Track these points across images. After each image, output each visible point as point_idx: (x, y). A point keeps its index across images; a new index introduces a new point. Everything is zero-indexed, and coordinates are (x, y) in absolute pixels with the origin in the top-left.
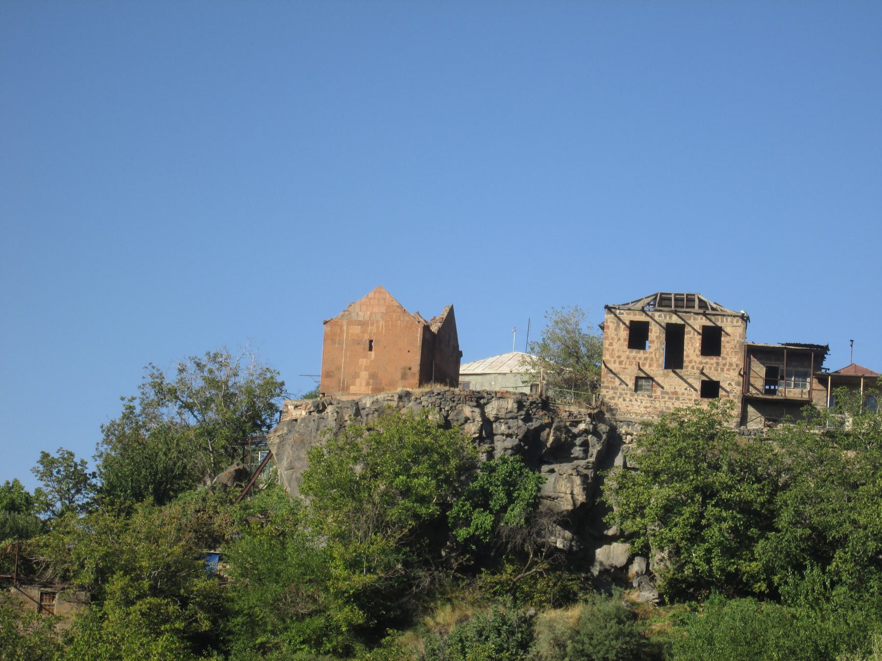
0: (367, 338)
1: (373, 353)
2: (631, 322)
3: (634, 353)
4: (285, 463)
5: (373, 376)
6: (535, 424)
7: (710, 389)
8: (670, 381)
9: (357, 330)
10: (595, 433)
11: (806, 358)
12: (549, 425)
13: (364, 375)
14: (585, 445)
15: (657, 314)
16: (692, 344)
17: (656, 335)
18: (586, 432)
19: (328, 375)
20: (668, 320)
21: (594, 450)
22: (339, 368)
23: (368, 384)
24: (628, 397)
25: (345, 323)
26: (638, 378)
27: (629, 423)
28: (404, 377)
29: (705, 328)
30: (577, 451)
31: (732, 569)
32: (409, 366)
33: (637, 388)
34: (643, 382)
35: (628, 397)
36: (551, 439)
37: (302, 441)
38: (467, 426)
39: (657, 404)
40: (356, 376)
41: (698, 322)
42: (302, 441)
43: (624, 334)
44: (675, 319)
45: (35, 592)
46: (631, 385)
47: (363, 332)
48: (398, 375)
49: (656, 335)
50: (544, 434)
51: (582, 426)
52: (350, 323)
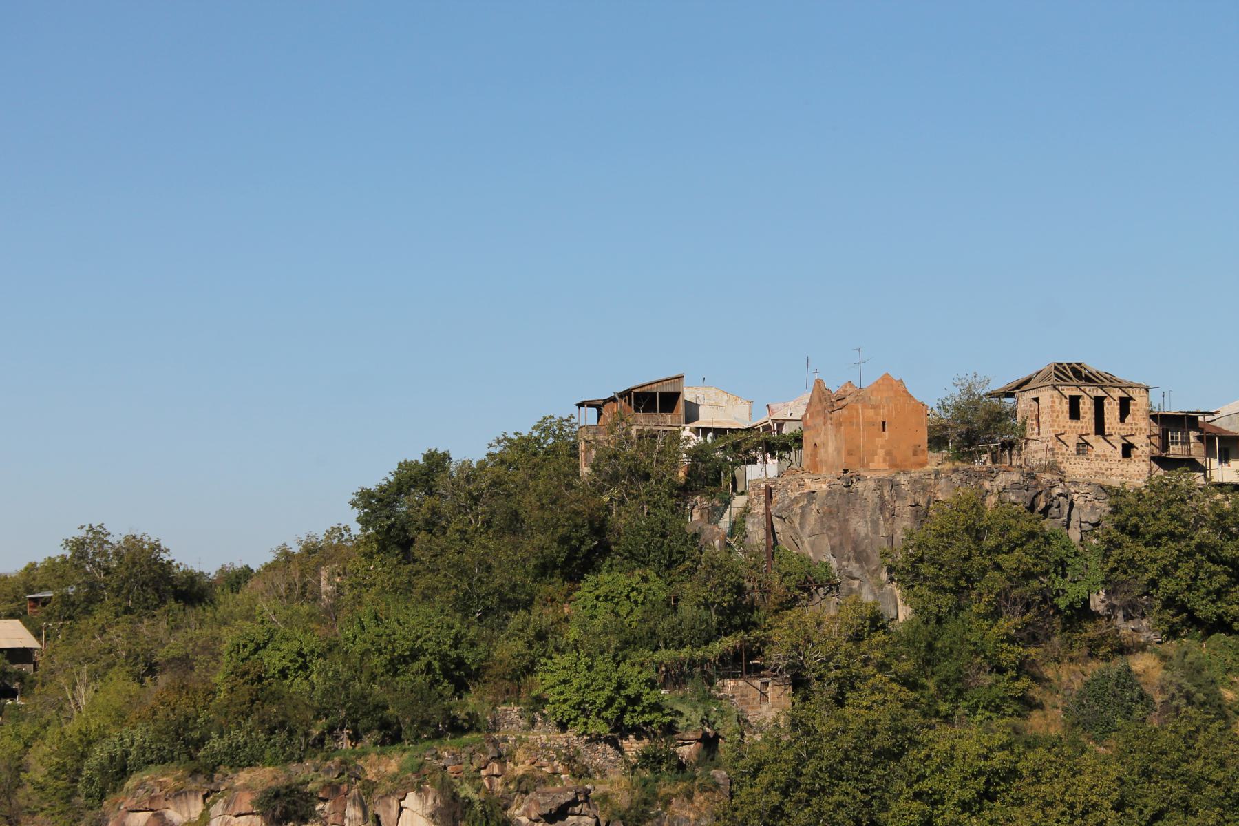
0: (880, 420)
1: (886, 433)
2: (1071, 397)
3: (1074, 423)
4: (807, 530)
5: (888, 453)
6: (1032, 493)
7: (1127, 450)
8: (1099, 445)
9: (871, 412)
10: (1066, 497)
11: (1187, 421)
12: (1040, 493)
13: (881, 452)
14: (1059, 506)
15: (1087, 389)
16: (1112, 411)
17: (1087, 407)
18: (1060, 495)
19: (850, 453)
20: (1096, 394)
21: (1067, 508)
22: (859, 447)
23: (885, 460)
24: (1073, 461)
25: (860, 406)
26: (1078, 444)
27: (1075, 483)
28: (915, 454)
29: (1121, 399)
30: (1054, 511)
31: (1220, 611)
32: (917, 443)
33: (1078, 453)
34: (1083, 447)
35: (1073, 461)
36: (1043, 505)
37: (831, 513)
38: (987, 498)
39: (1093, 466)
40: (874, 453)
41: (1117, 394)
42: (831, 513)
43: (1066, 407)
44: (1100, 393)
45: (757, 683)
46: (1073, 449)
47: (877, 414)
48: (910, 453)
49: (1087, 407)
50: (1037, 499)
51: (1057, 491)
52: (864, 407)
